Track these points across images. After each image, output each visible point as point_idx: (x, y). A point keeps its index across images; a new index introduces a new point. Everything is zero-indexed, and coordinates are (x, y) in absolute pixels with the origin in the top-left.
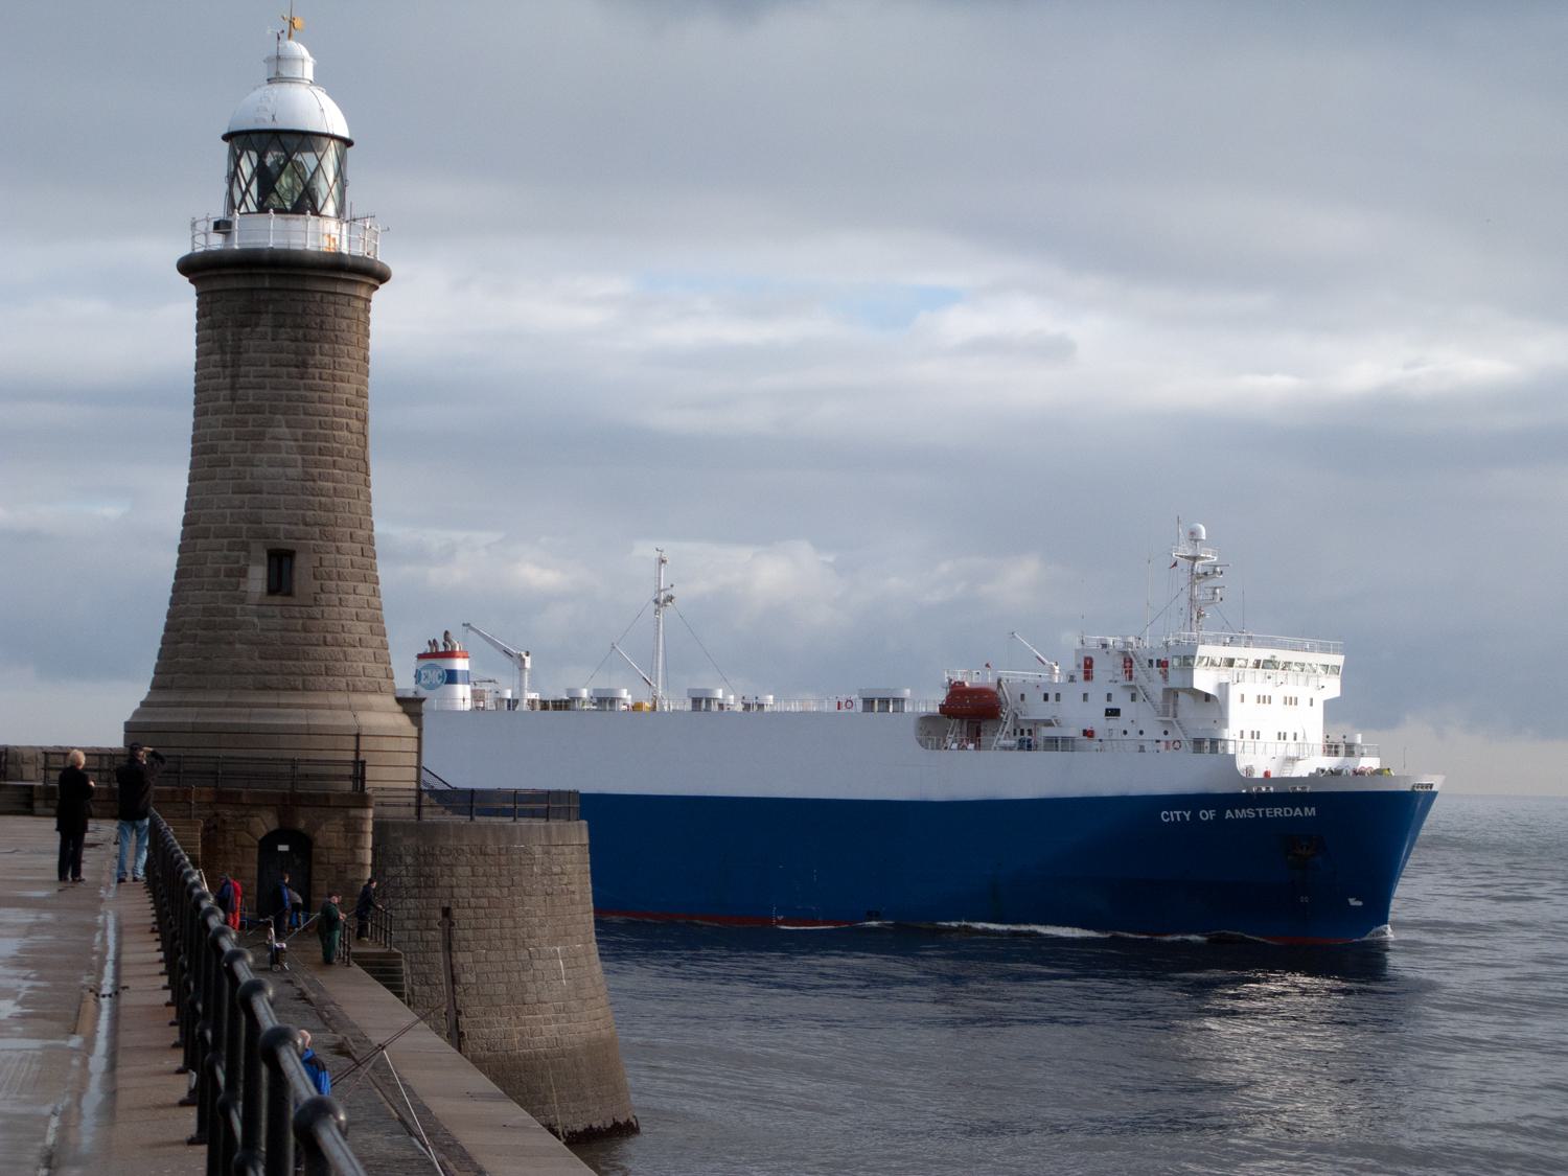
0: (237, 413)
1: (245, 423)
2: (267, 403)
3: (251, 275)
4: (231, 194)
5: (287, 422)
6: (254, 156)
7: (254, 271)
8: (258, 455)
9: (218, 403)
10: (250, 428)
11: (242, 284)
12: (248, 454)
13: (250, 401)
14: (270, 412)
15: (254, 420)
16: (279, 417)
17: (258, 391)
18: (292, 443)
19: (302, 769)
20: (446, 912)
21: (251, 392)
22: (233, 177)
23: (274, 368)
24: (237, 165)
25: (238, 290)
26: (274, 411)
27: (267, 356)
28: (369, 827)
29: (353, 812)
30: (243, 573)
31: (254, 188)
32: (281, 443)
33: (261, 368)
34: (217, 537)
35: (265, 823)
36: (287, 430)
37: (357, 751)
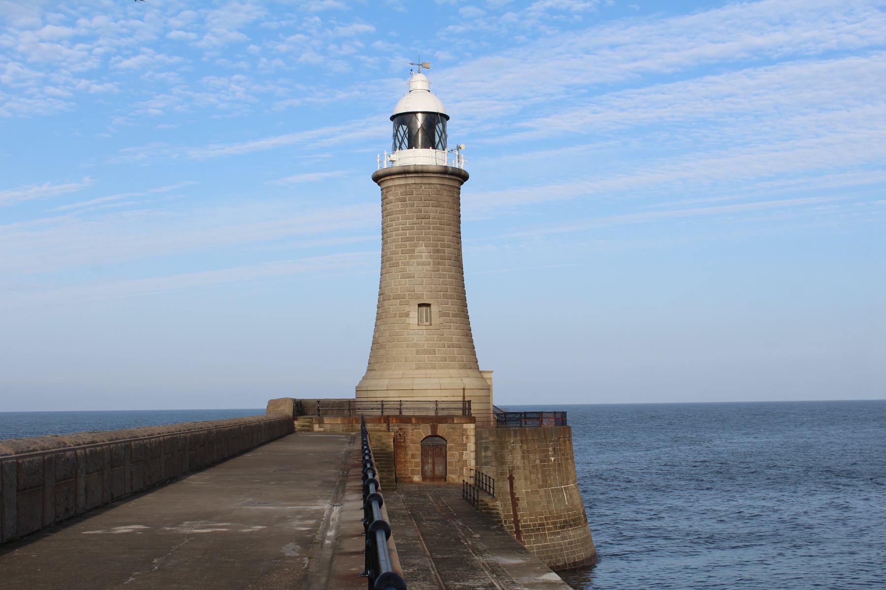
1: (406, 246)
4: (395, 143)
6: (405, 127)
11: (402, 182)
19: (440, 406)
20: (511, 471)
22: (395, 136)
24: (397, 130)
26: (419, 239)
28: (471, 433)
29: (465, 426)
30: (407, 315)
31: (406, 141)
34: (394, 299)
35: (424, 431)
37: (464, 397)
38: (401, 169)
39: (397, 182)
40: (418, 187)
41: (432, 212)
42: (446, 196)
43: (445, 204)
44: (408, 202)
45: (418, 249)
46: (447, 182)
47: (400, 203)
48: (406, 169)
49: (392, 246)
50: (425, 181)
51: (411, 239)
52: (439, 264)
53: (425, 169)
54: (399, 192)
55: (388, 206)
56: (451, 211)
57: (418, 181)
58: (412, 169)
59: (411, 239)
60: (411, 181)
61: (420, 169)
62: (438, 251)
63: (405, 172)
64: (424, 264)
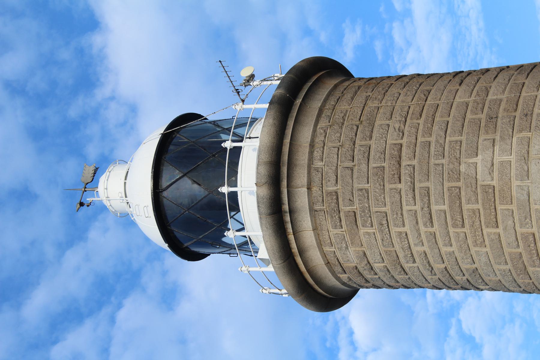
0: (463, 226)
1: (475, 213)
2: (447, 185)
3: (291, 212)
5: (470, 156)
7: (286, 207)
8: (514, 193)
9: (457, 254)
10: (480, 206)
11: (305, 222)
12: (514, 207)
13: (446, 207)
14: (459, 180)
15: (469, 201)
16: (463, 168)
17: (432, 199)
18: (497, 148)
21: (435, 208)
23: (403, 178)
25: (315, 229)
26: (456, 175)
27: (388, 186)
32: (497, 159)
33: (403, 193)
36: (480, 157)
38: (268, 220)
39: (309, 237)
40: (316, 178)
41: (386, 134)
42: (349, 106)
43: (372, 104)
44: (356, 206)
45: (483, 178)
46: (316, 104)
47: (362, 231)
48: (265, 210)
49: (482, 255)
50: (302, 157)
51: (456, 197)
52: (528, 115)
53: (266, 157)
54: (334, 232)
55: (376, 266)
56: (393, 90)
57: (301, 177)
58: (265, 191)
59: (456, 197)
60: (302, 199)
61: (264, 170)
62: (492, 119)
63: (278, 213)
64: (525, 158)
